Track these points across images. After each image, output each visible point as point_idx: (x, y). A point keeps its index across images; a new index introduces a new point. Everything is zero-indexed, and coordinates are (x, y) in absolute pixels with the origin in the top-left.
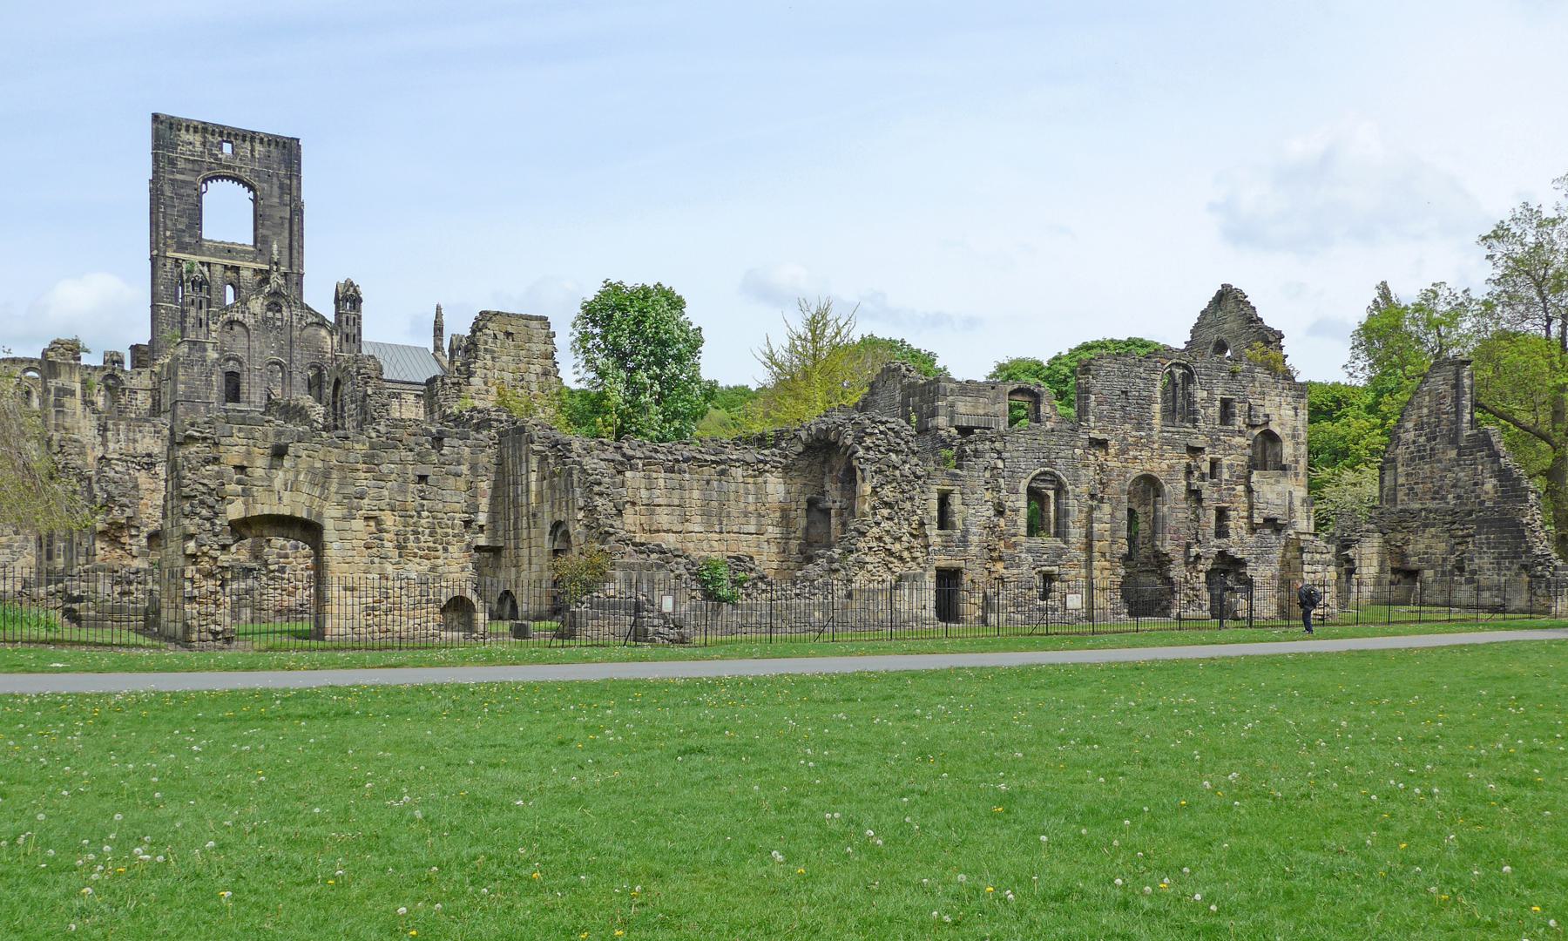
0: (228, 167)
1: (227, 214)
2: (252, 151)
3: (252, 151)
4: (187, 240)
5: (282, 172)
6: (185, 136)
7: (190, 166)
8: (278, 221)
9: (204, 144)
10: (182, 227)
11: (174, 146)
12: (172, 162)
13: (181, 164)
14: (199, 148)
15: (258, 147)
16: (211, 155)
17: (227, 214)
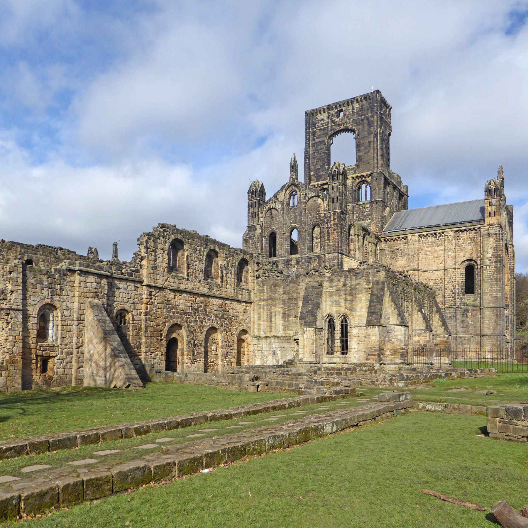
0: (341, 125)
1: (343, 151)
2: (353, 109)
3: (353, 109)
4: (321, 173)
5: (369, 115)
6: (320, 117)
7: (322, 132)
8: (367, 144)
9: (328, 117)
10: (319, 167)
11: (314, 125)
12: (314, 134)
13: (317, 134)
14: (326, 120)
15: (356, 105)
16: (333, 121)
17: (343, 151)
